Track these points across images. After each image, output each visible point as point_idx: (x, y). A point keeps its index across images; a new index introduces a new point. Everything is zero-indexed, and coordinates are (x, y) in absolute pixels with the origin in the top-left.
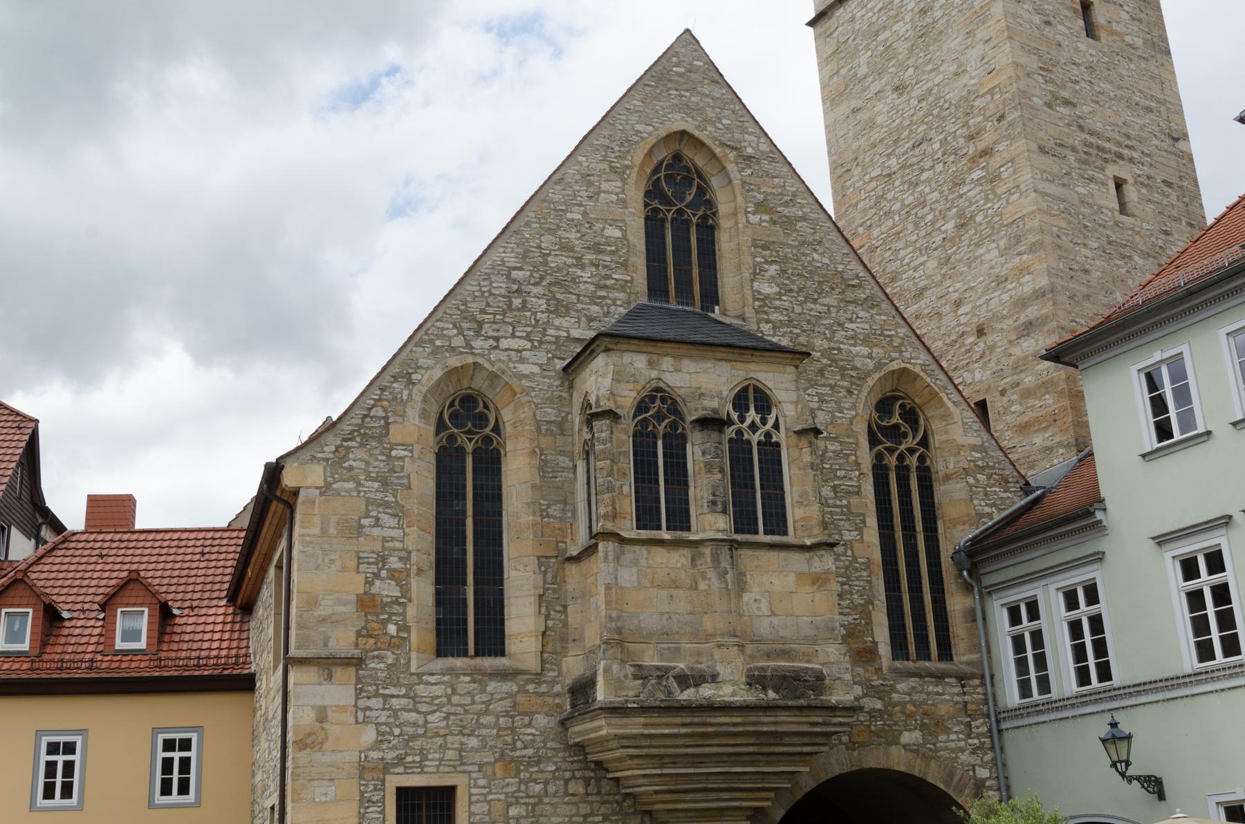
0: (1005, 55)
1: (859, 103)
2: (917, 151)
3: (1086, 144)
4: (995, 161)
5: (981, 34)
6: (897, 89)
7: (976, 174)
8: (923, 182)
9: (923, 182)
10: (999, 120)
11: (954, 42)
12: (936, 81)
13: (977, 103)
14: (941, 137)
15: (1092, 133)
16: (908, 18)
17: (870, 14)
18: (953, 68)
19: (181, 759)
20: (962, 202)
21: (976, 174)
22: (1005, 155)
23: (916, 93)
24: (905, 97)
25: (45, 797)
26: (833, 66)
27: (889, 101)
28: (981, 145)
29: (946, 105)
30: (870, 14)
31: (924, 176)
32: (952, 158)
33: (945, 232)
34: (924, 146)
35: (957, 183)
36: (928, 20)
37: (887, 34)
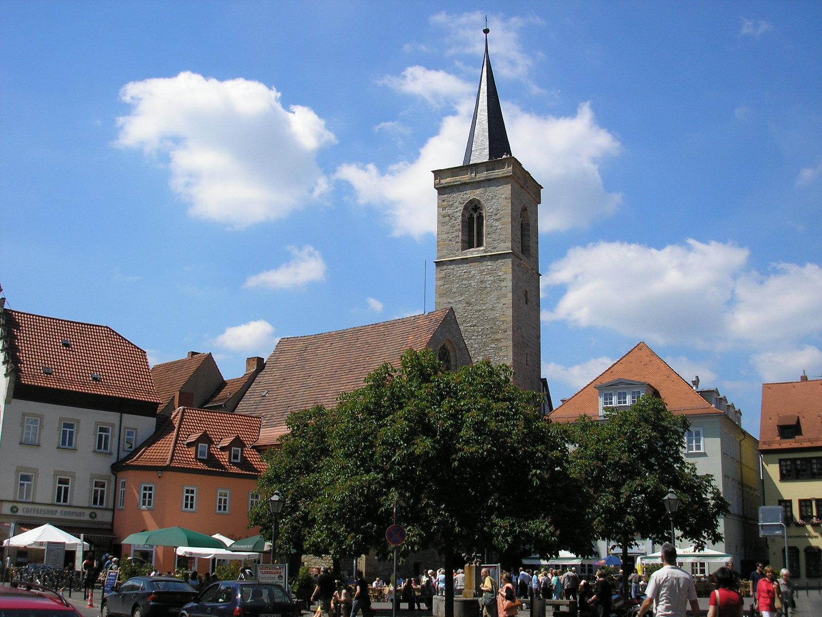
0: (510, 312)
1: (452, 301)
2: (472, 328)
3: (523, 342)
4: (501, 345)
5: (503, 301)
6: (467, 303)
7: (493, 346)
8: (473, 339)
9: (473, 339)
10: (504, 332)
11: (493, 297)
12: (484, 308)
13: (497, 322)
14: (482, 327)
15: (524, 338)
16: (476, 281)
17: (461, 271)
18: (491, 307)
19: (224, 499)
20: (486, 353)
21: (493, 346)
22: (504, 344)
23: (475, 308)
24: (470, 308)
25: (185, 508)
26: (440, 283)
27: (464, 305)
28: (497, 337)
29: (486, 318)
30: (461, 271)
31: (474, 338)
32: (485, 336)
33: (478, 359)
34: (475, 327)
35: (485, 345)
36: (483, 286)
37: (466, 282)
